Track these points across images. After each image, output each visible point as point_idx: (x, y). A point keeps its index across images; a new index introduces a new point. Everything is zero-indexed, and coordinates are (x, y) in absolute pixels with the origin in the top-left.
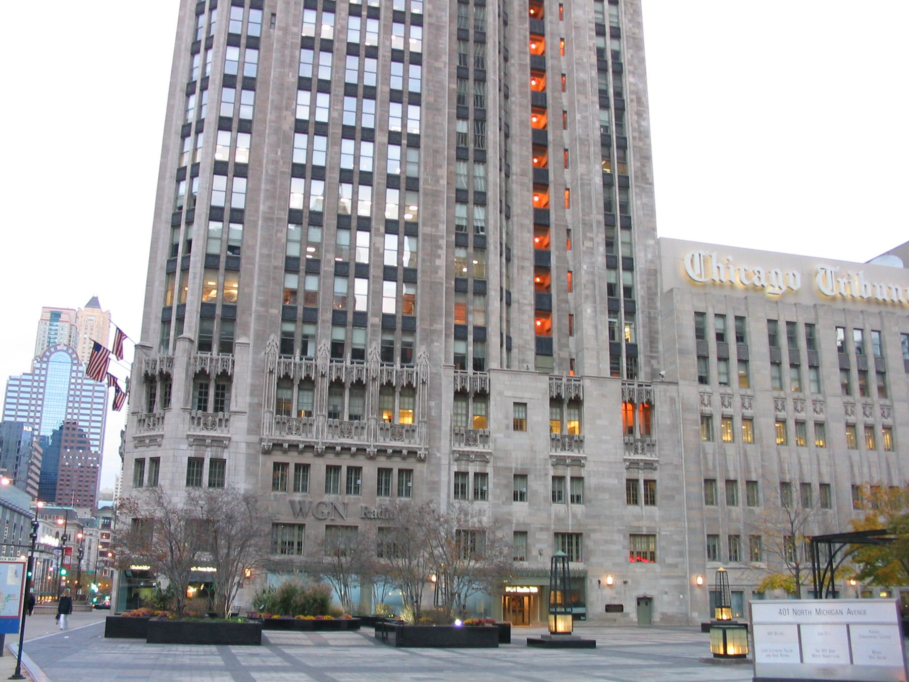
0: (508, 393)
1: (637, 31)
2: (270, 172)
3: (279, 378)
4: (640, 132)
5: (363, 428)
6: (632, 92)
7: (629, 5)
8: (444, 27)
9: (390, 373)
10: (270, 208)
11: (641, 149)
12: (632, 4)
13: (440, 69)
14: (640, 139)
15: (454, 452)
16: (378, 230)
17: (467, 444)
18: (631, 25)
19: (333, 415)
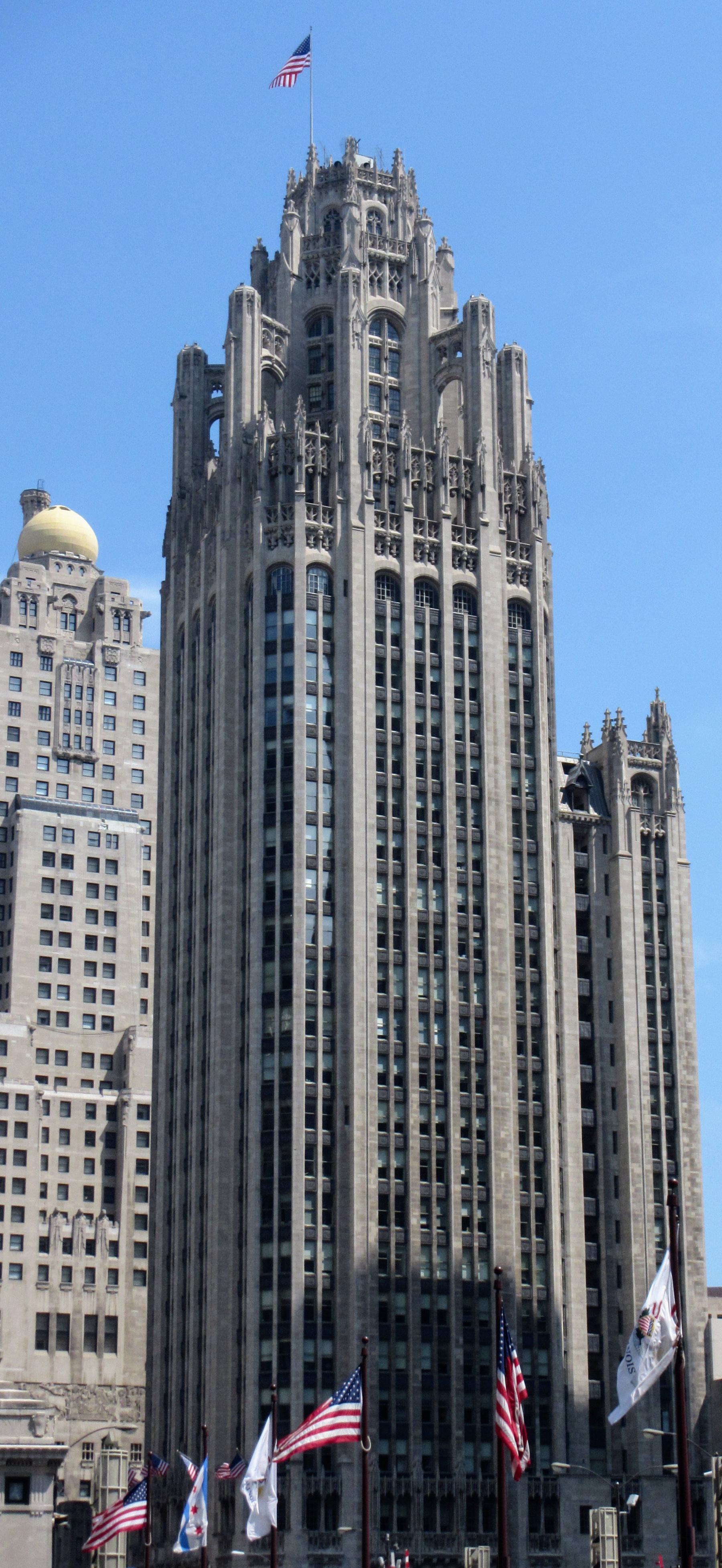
0: (575, 1498)
1: (690, 1078)
2: (360, 1288)
3: (382, 1496)
4: (693, 1201)
5: (453, 1540)
6: (686, 1155)
7: (684, 1047)
8: (508, 1110)
9: (475, 1486)
10: (363, 1325)
11: (694, 1220)
12: (687, 1044)
13: (505, 1160)
14: (694, 1209)
15: (530, 1558)
16: (457, 1341)
17: (541, 1549)
18: (685, 1072)
19: (428, 1525)
